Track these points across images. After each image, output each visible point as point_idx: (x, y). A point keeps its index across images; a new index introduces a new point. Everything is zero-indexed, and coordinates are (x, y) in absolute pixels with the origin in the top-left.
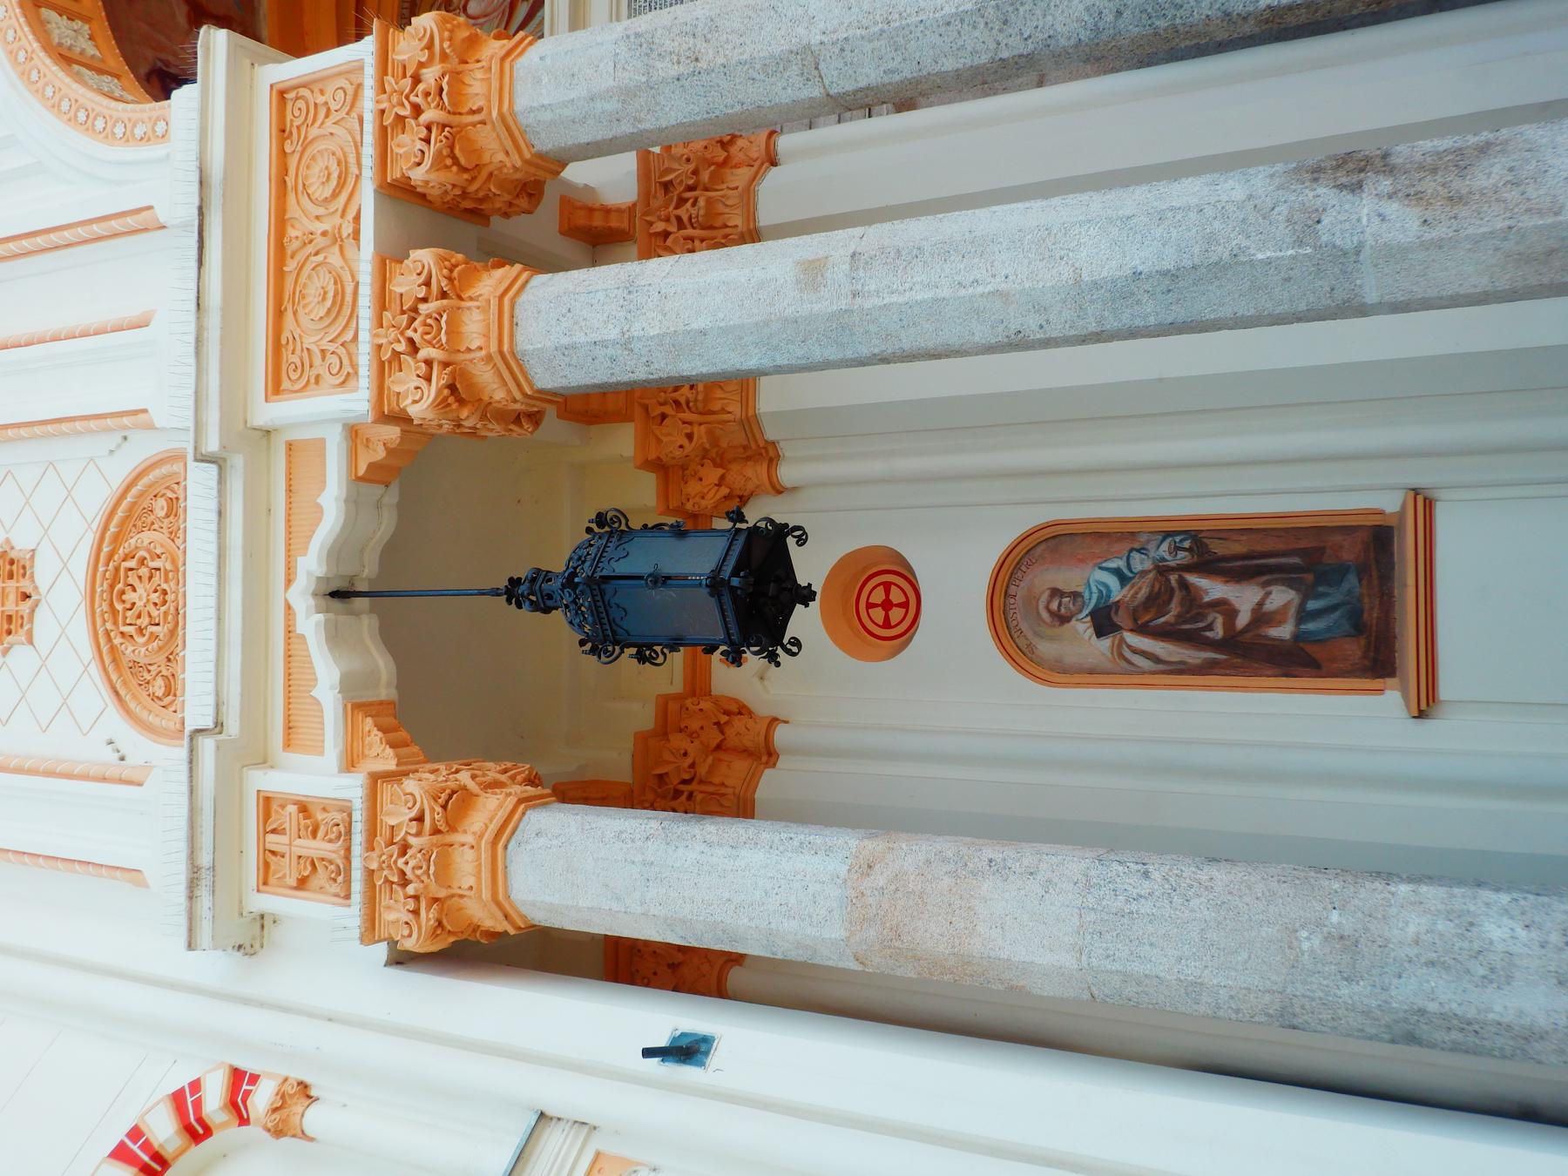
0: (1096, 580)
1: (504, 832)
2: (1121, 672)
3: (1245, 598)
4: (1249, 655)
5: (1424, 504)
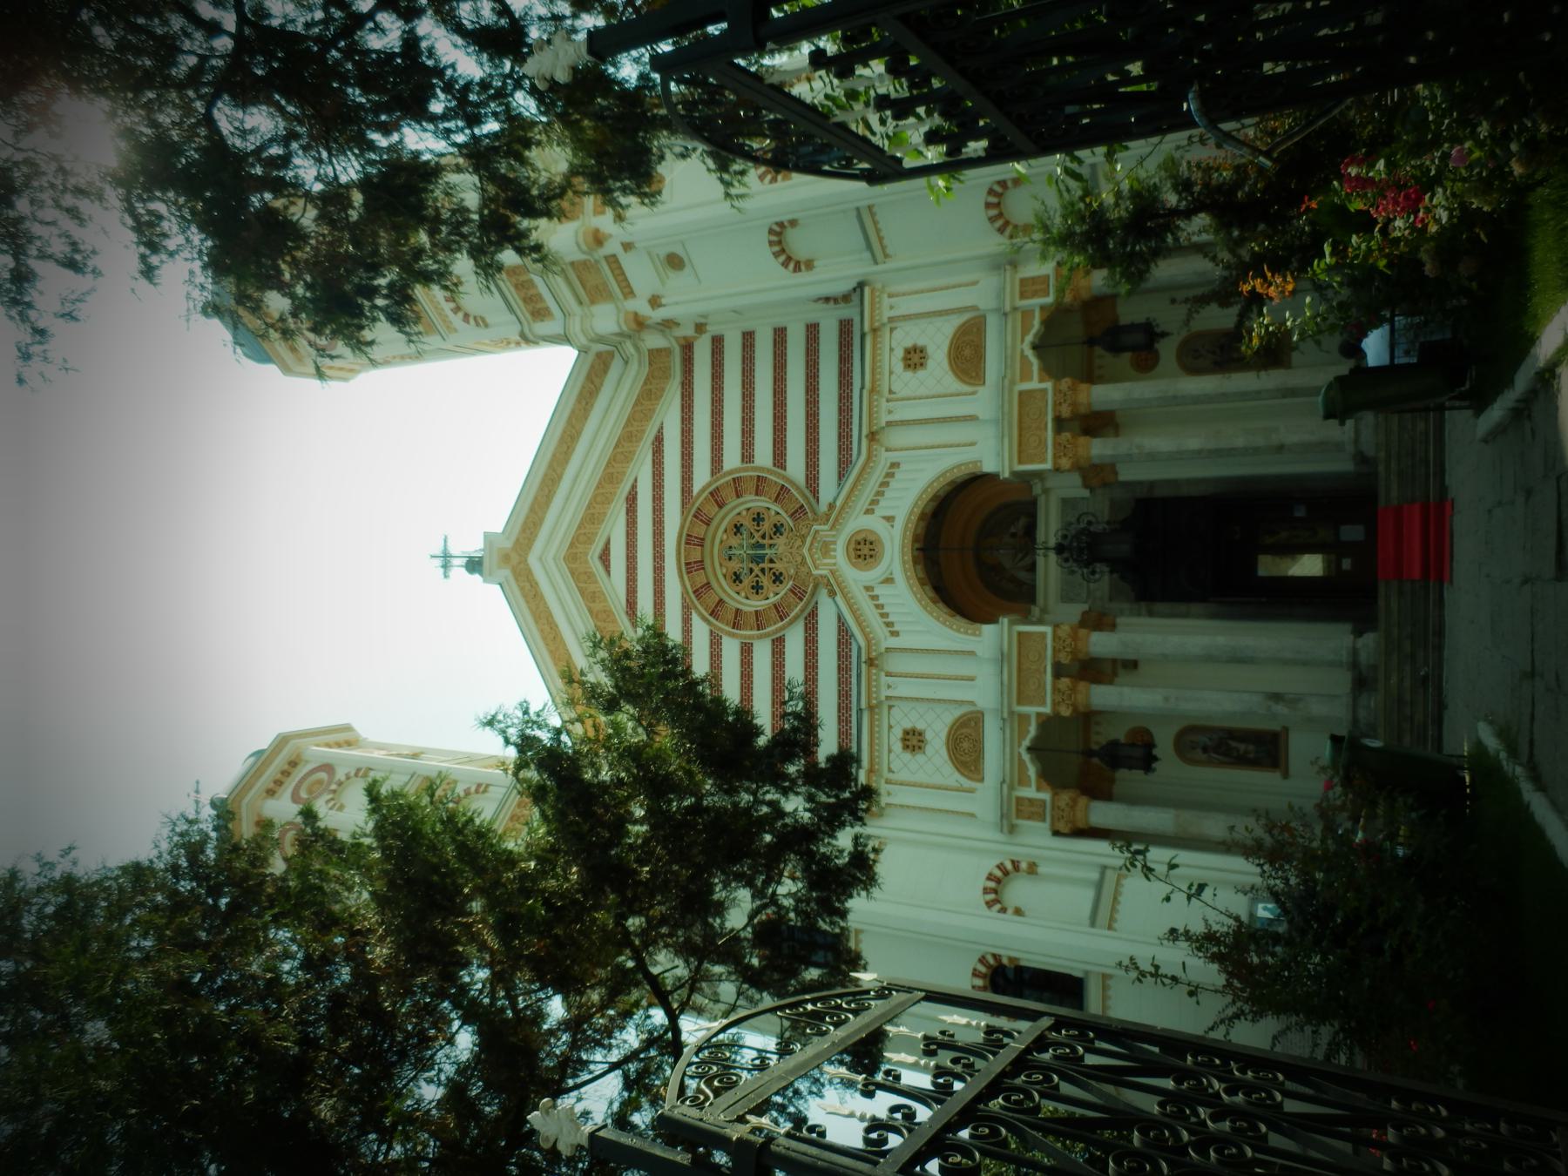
0: (1203, 739)
1: (1087, 807)
2: (1209, 763)
3: (1242, 747)
4: (1243, 761)
5: (1286, 729)
